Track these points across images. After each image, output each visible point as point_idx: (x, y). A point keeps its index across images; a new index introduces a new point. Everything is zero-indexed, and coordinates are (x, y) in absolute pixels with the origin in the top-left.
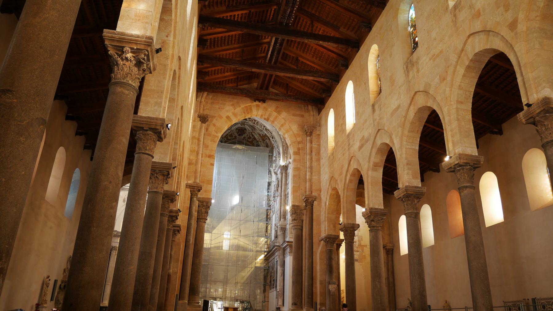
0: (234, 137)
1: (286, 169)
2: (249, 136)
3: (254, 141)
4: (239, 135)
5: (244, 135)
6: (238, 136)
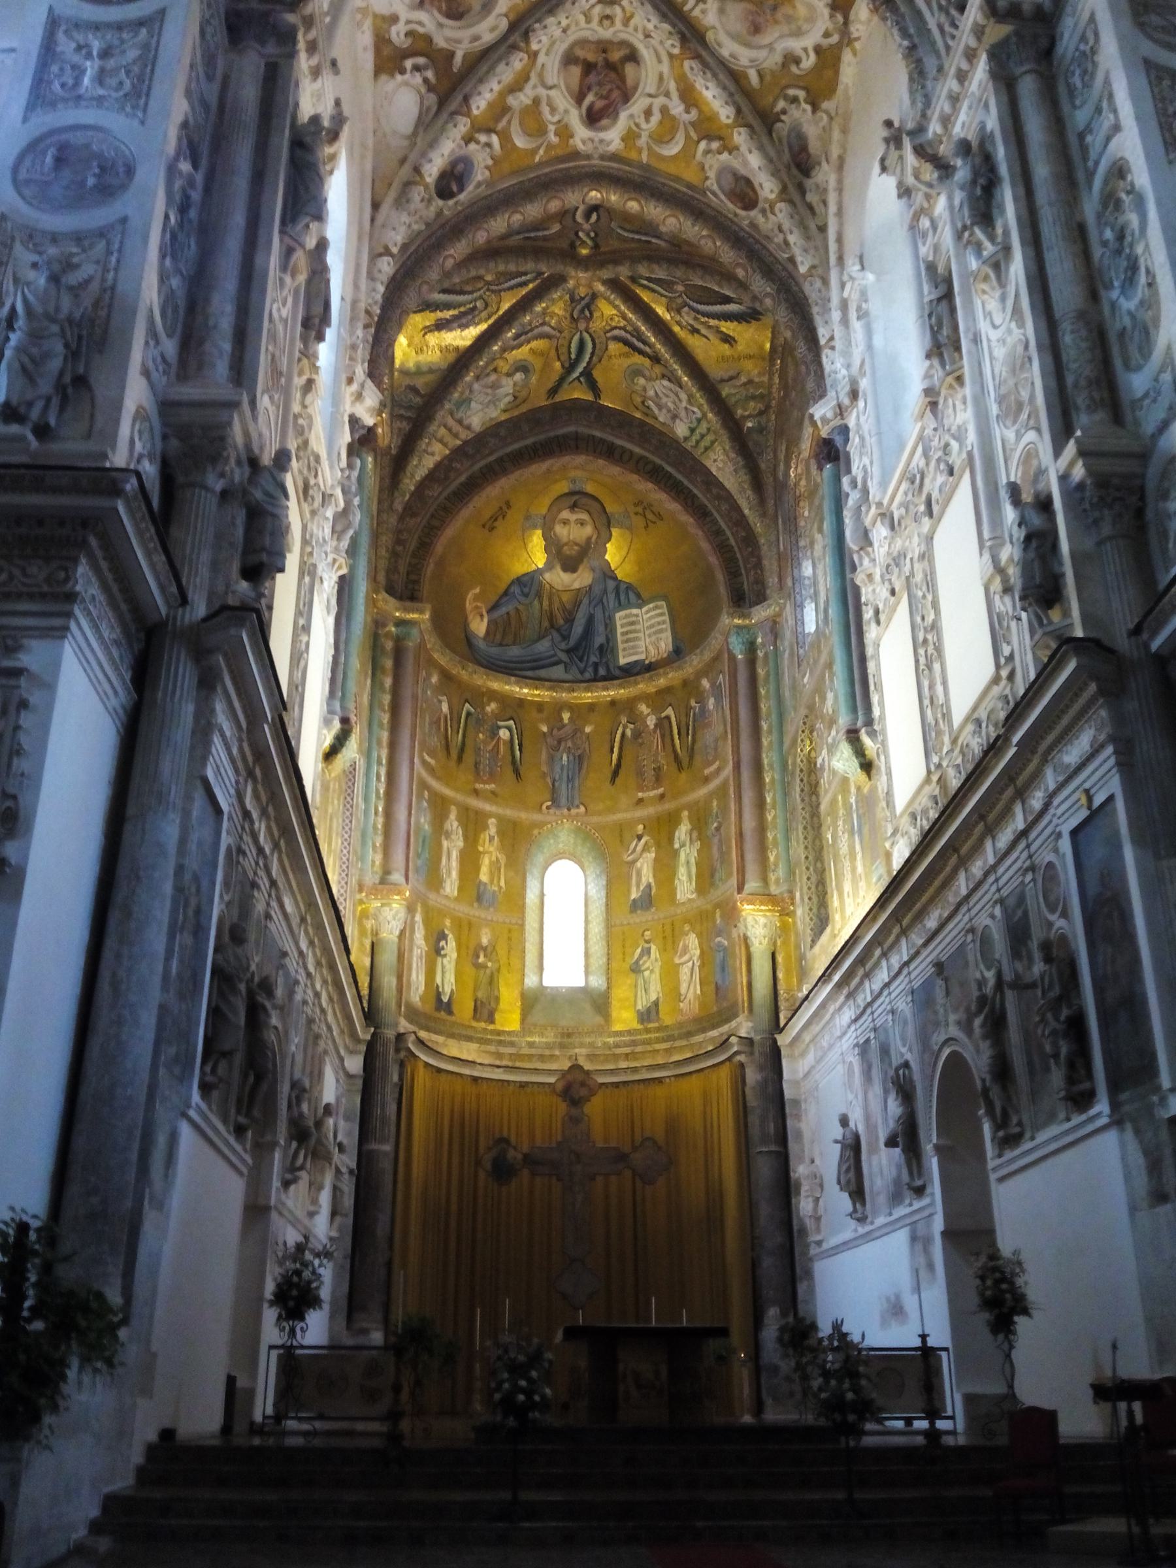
0: (556, 134)
1: (1044, 42)
2: (664, 110)
3: (703, 145)
4: (593, 118)
5: (623, 116)
6: (581, 134)
